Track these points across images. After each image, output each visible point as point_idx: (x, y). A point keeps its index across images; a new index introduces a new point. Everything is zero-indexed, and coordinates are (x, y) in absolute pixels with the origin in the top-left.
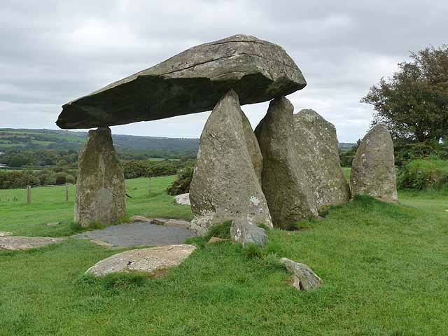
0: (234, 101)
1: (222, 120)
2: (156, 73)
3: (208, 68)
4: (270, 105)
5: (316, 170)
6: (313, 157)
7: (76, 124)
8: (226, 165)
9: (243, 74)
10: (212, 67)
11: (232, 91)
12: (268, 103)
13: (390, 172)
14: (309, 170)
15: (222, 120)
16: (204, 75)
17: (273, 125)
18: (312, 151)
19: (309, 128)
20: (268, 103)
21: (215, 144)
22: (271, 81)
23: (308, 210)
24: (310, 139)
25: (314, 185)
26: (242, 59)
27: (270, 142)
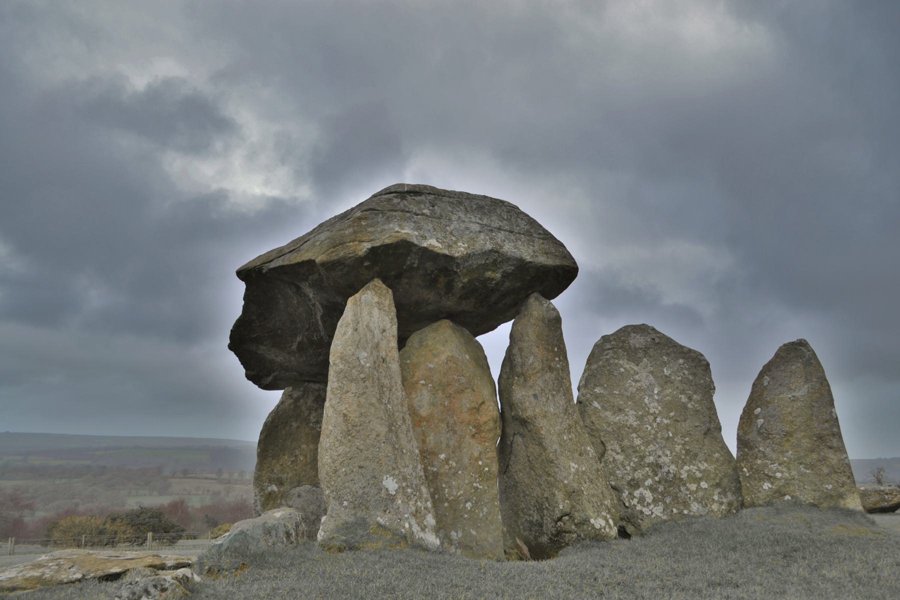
0: (376, 299)
2: (254, 264)
5: (647, 443)
6: (640, 418)
8: (345, 416)
11: (378, 282)
13: (830, 448)
14: (626, 443)
18: (639, 405)
23: (585, 521)
25: (638, 475)
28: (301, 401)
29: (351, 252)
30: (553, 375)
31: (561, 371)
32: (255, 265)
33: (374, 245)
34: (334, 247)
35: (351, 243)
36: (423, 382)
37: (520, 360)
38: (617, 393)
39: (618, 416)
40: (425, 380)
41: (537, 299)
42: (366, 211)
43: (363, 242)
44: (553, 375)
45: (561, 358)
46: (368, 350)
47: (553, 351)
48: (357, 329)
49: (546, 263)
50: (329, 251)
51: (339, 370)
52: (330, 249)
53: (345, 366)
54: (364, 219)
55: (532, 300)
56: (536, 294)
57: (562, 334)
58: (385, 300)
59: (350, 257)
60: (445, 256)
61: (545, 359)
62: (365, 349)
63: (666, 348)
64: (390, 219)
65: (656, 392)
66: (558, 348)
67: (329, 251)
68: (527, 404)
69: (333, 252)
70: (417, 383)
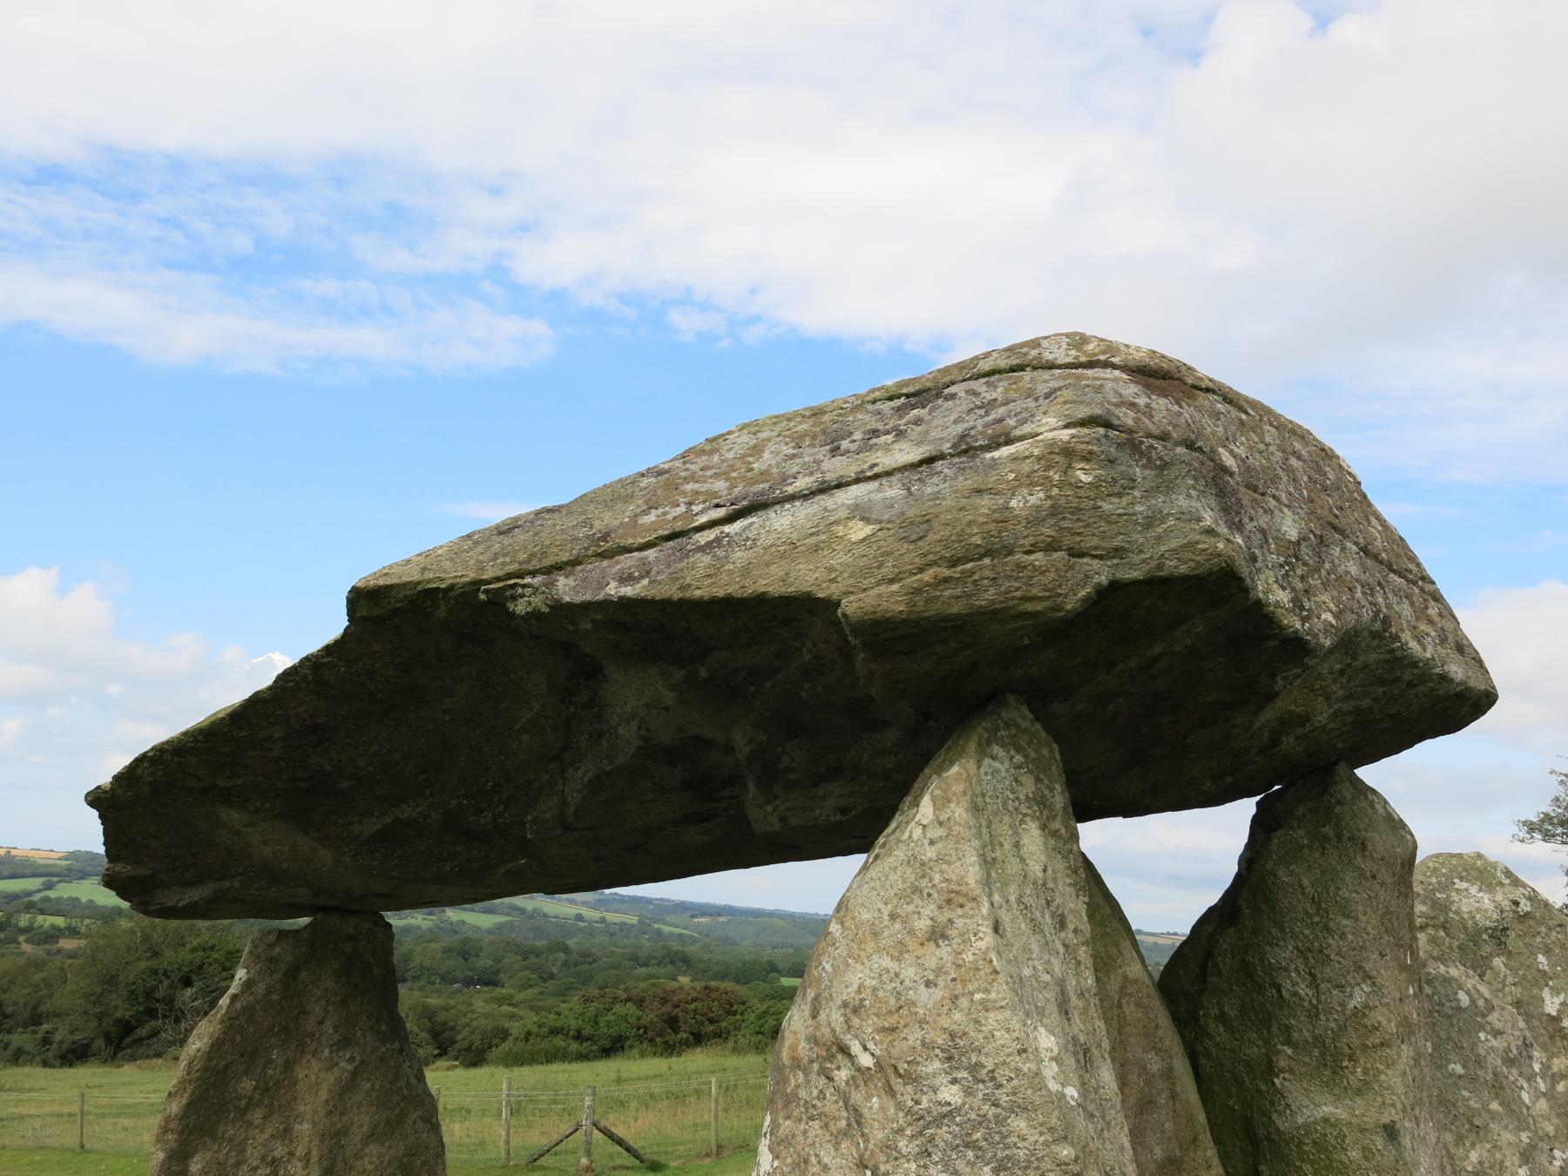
0: (1028, 787)
1: (937, 935)
2: (460, 573)
3: (819, 541)
4: (1261, 826)
7: (193, 895)
9: (1102, 574)
10: (860, 512)
11: (1019, 714)
12: (1244, 810)
15: (937, 935)
16: (806, 577)
17: (1283, 954)
18: (1517, 1116)
19: (1480, 967)
20: (1244, 810)
21: (878, 1135)
22: (1297, 647)
24: (1497, 1033)
26: (1088, 457)
27: (1270, 1070)
28: (303, 975)
29: (1035, 591)
32: (472, 575)
33: (1118, 575)
34: (954, 562)
35: (1039, 555)
37: (1303, 989)
38: (1459, 1070)
39: (1473, 1145)
42: (1082, 423)
43: (1081, 555)
50: (927, 576)
51: (936, 1110)
52: (934, 563)
53: (968, 1092)
54: (1084, 459)
59: (1026, 615)
63: (1543, 929)
64: (1172, 473)
65: (1537, 1067)
67: (927, 576)
68: (1354, 1154)
69: (946, 580)
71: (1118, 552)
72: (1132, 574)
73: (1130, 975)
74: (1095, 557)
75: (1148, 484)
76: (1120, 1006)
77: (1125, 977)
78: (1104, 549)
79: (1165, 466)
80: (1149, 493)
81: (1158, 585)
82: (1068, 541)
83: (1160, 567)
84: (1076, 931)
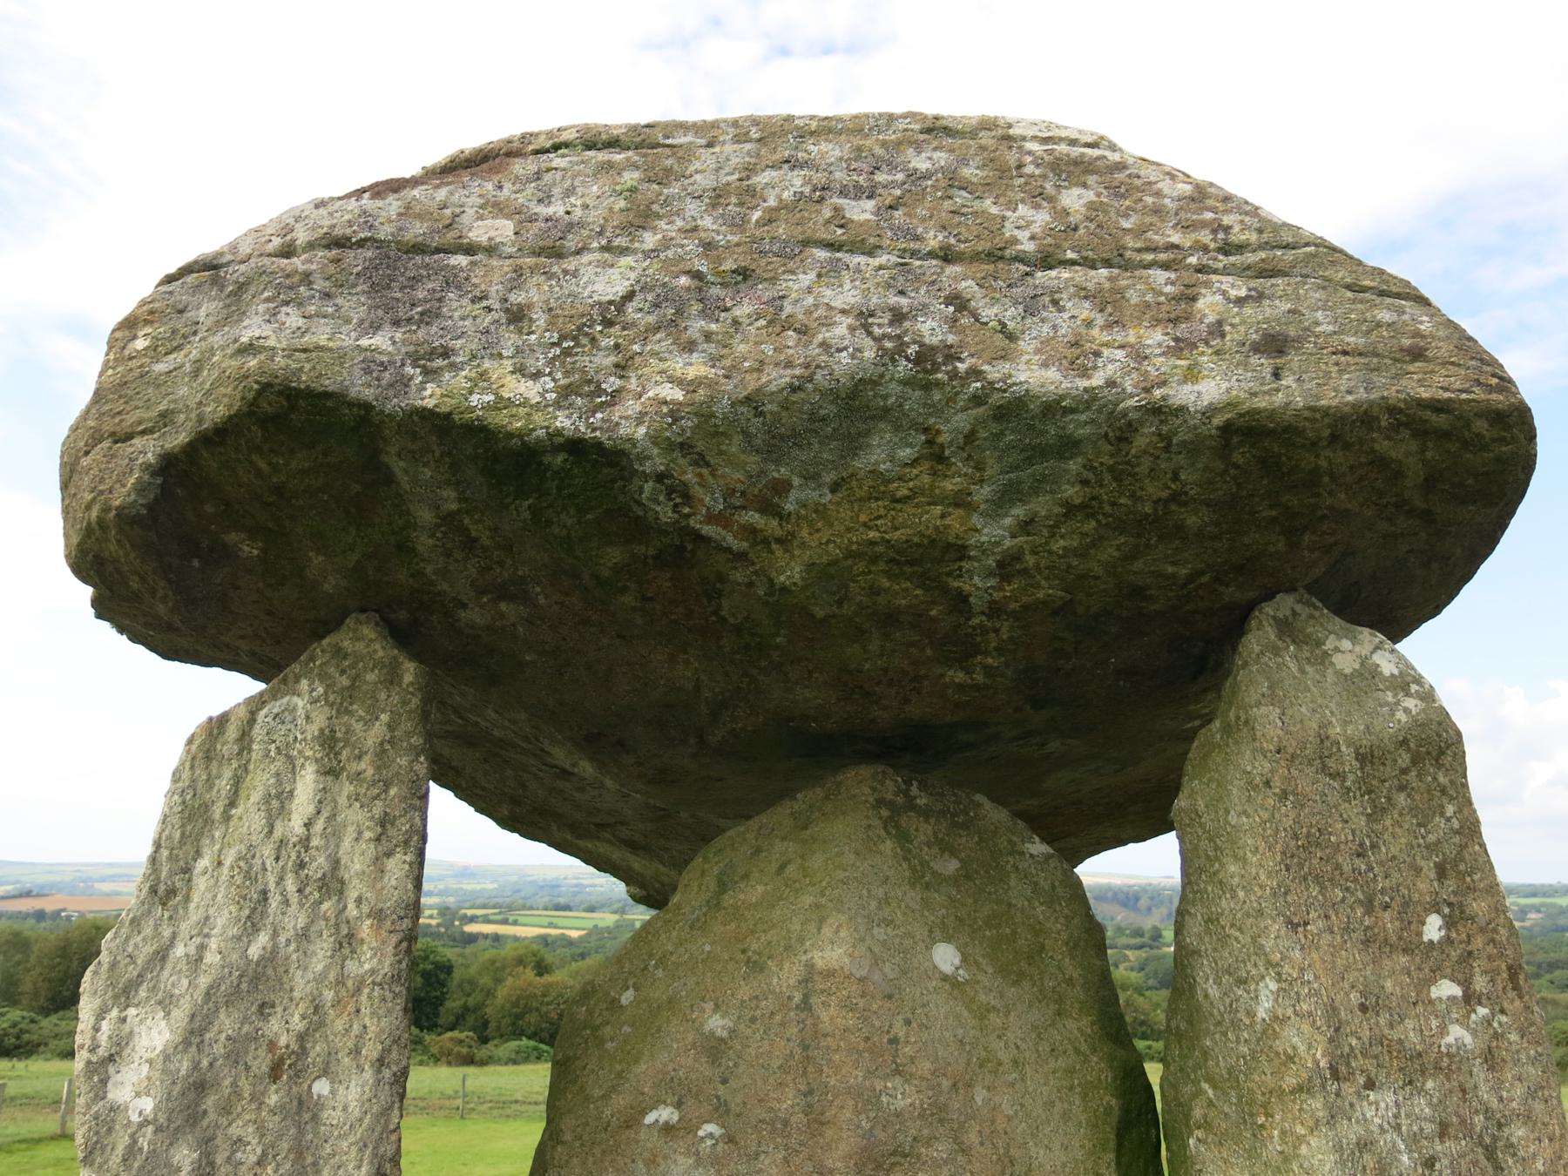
9: (148, 450)
30: (1421, 1106)
31: (1480, 1072)
33: (168, 446)
36: (664, 1114)
40: (679, 1105)
41: (1286, 628)
43: (129, 437)
44: (1421, 1106)
45: (1480, 984)
46: (180, 1014)
47: (1412, 945)
48: (172, 892)
49: (1261, 403)
54: (147, 322)
55: (1258, 638)
56: (1285, 604)
57: (1470, 828)
58: (368, 724)
60: (576, 447)
61: (1355, 997)
62: (166, 1003)
66: (1449, 923)
70: (632, 1121)
71: (166, 417)
72: (178, 439)
73: (820, 964)
74: (143, 433)
75: (209, 322)
76: (805, 1006)
77: (810, 966)
78: (150, 419)
79: (241, 287)
80: (219, 325)
81: (213, 439)
82: (107, 428)
83: (200, 420)
84: (359, 901)
